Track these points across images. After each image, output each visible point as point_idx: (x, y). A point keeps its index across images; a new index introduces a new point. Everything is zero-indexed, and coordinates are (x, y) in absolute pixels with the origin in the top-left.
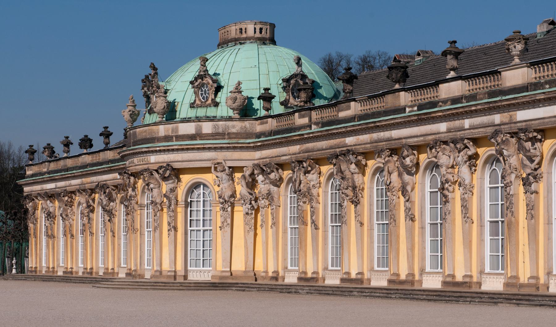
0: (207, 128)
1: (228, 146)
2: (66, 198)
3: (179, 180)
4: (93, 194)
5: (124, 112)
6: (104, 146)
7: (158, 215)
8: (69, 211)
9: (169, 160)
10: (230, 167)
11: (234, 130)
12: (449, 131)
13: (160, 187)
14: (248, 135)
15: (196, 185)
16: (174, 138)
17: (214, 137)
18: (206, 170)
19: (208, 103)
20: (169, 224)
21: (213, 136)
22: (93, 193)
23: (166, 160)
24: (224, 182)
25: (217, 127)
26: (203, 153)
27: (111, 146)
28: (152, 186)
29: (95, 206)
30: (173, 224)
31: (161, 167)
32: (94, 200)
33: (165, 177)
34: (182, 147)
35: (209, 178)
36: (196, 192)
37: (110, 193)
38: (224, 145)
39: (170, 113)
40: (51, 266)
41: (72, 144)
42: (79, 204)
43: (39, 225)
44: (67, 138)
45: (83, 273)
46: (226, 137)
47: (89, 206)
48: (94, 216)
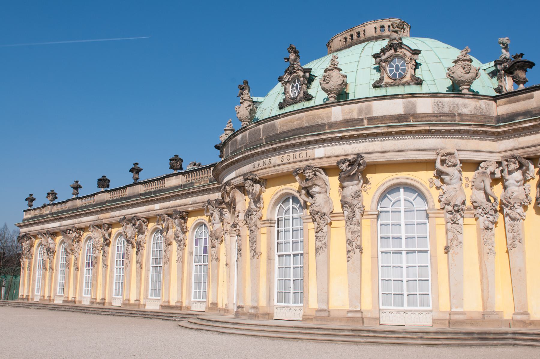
0: (424, 106)
1: (468, 128)
2: (74, 234)
3: (366, 182)
4: (110, 229)
5: (239, 108)
6: (133, 181)
7: (325, 229)
8: (75, 246)
9: (356, 152)
10: (461, 161)
11: (466, 111)
13: (326, 192)
14: (488, 118)
15: (394, 188)
16: (365, 122)
17: (439, 118)
18: (429, 164)
19: (404, 80)
20: (349, 242)
21: (437, 116)
22: (109, 228)
23: (350, 152)
24: (454, 181)
25: (440, 105)
26: (422, 140)
27: (141, 180)
28: (316, 189)
29: (111, 240)
30: (358, 243)
31: (343, 162)
32: (110, 235)
33: (349, 176)
34: (390, 130)
35: (423, 178)
36: (393, 197)
37: (140, 225)
38: (462, 128)
39: (341, 96)
40: (47, 295)
41: (81, 187)
42: (89, 238)
43: (33, 260)
44: (77, 182)
45: (92, 303)
46: (457, 118)
47: (105, 240)
48: (110, 249)
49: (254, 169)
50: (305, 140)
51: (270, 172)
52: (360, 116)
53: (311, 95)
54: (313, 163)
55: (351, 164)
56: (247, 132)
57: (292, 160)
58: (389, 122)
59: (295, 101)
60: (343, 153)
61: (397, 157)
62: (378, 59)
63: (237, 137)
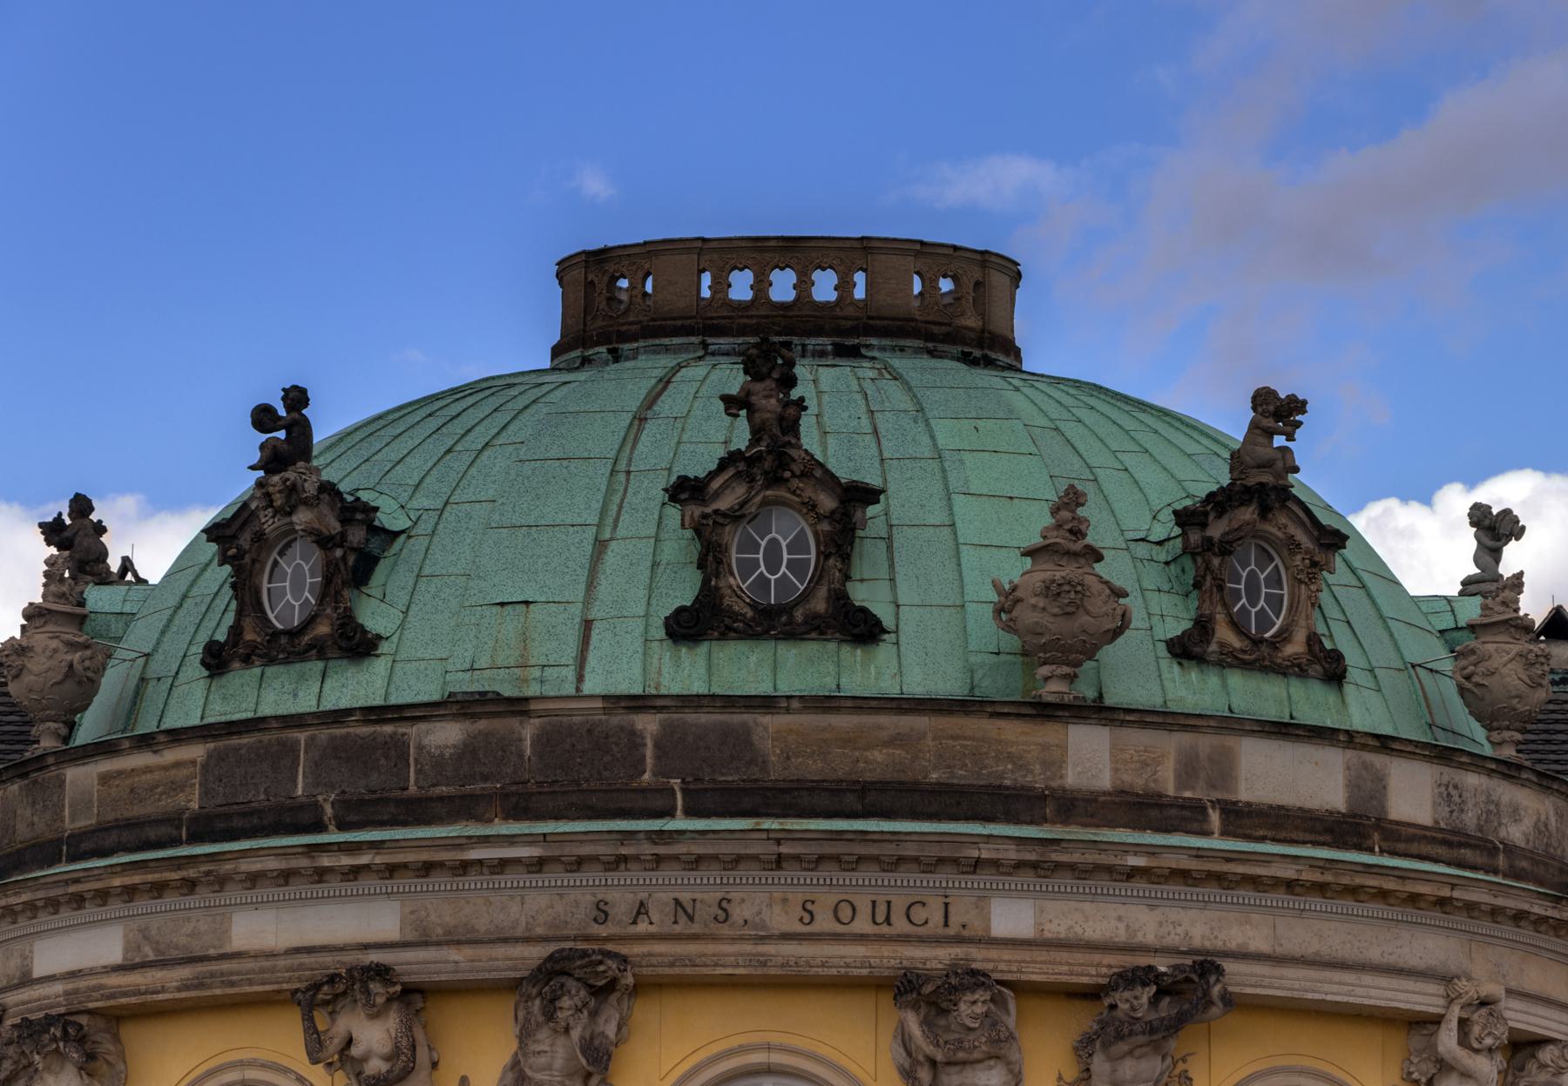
0: (1412, 795)
16: (1215, 818)
21: (1449, 844)
23: (1149, 936)
31: (1144, 976)
49: (603, 931)
50: (975, 854)
51: (730, 955)
52: (1186, 789)
53: (878, 622)
54: (980, 957)
55: (1166, 989)
56: (528, 731)
57: (862, 925)
58: (1301, 836)
60: (1122, 936)
61: (1326, 987)
62: (1195, 537)
63: (413, 731)
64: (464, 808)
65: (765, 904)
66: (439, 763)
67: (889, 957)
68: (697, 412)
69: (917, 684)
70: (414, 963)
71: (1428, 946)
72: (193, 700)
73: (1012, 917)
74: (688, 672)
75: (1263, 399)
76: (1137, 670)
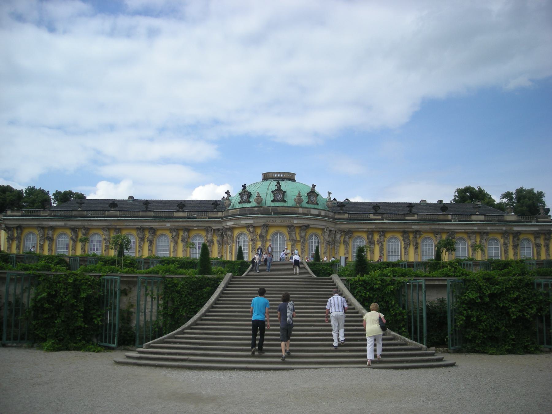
0: (323, 213)
12: (478, 229)
20: (302, 249)
51: (276, 224)
55: (306, 226)
59: (279, 201)
64: (258, 214)
65: (278, 221)
66: (256, 211)
67: (287, 224)
68: (273, 185)
69: (289, 205)
70: (254, 225)
71: (324, 224)
72: (238, 206)
73: (295, 221)
74: (273, 204)
75: (313, 185)
76: (304, 204)
